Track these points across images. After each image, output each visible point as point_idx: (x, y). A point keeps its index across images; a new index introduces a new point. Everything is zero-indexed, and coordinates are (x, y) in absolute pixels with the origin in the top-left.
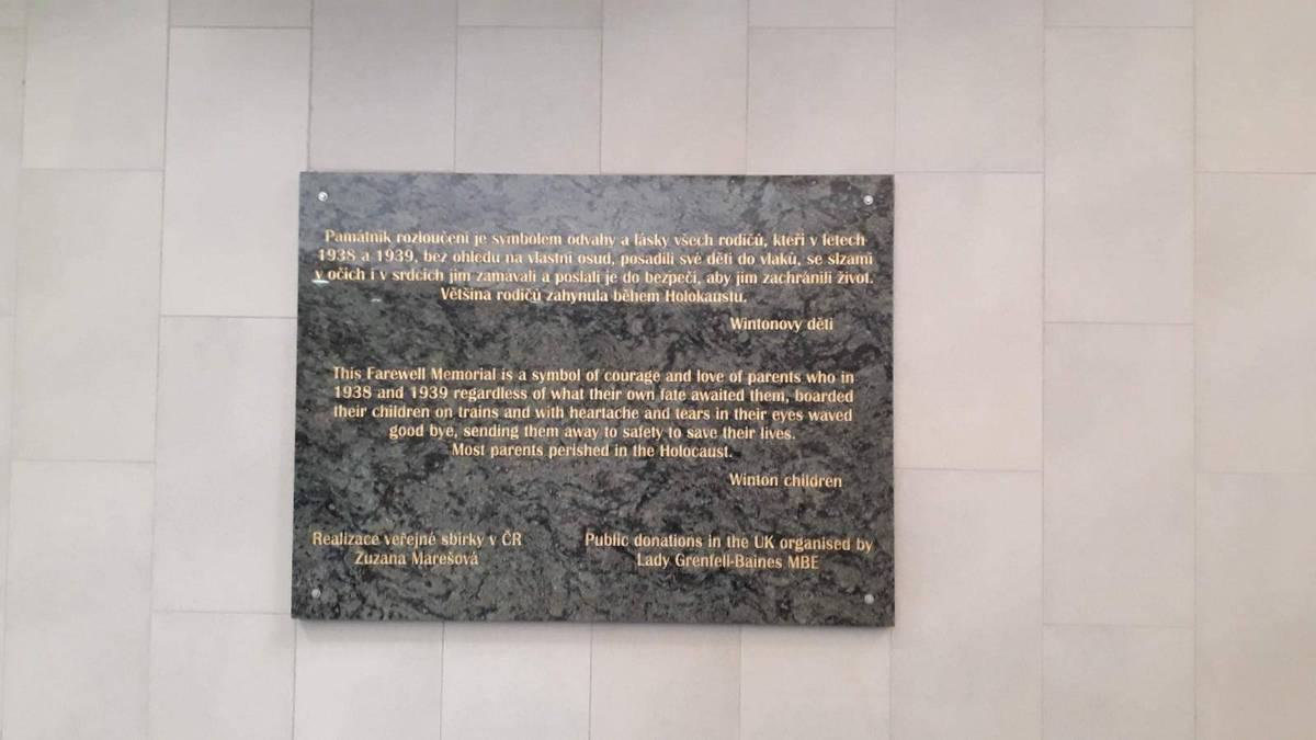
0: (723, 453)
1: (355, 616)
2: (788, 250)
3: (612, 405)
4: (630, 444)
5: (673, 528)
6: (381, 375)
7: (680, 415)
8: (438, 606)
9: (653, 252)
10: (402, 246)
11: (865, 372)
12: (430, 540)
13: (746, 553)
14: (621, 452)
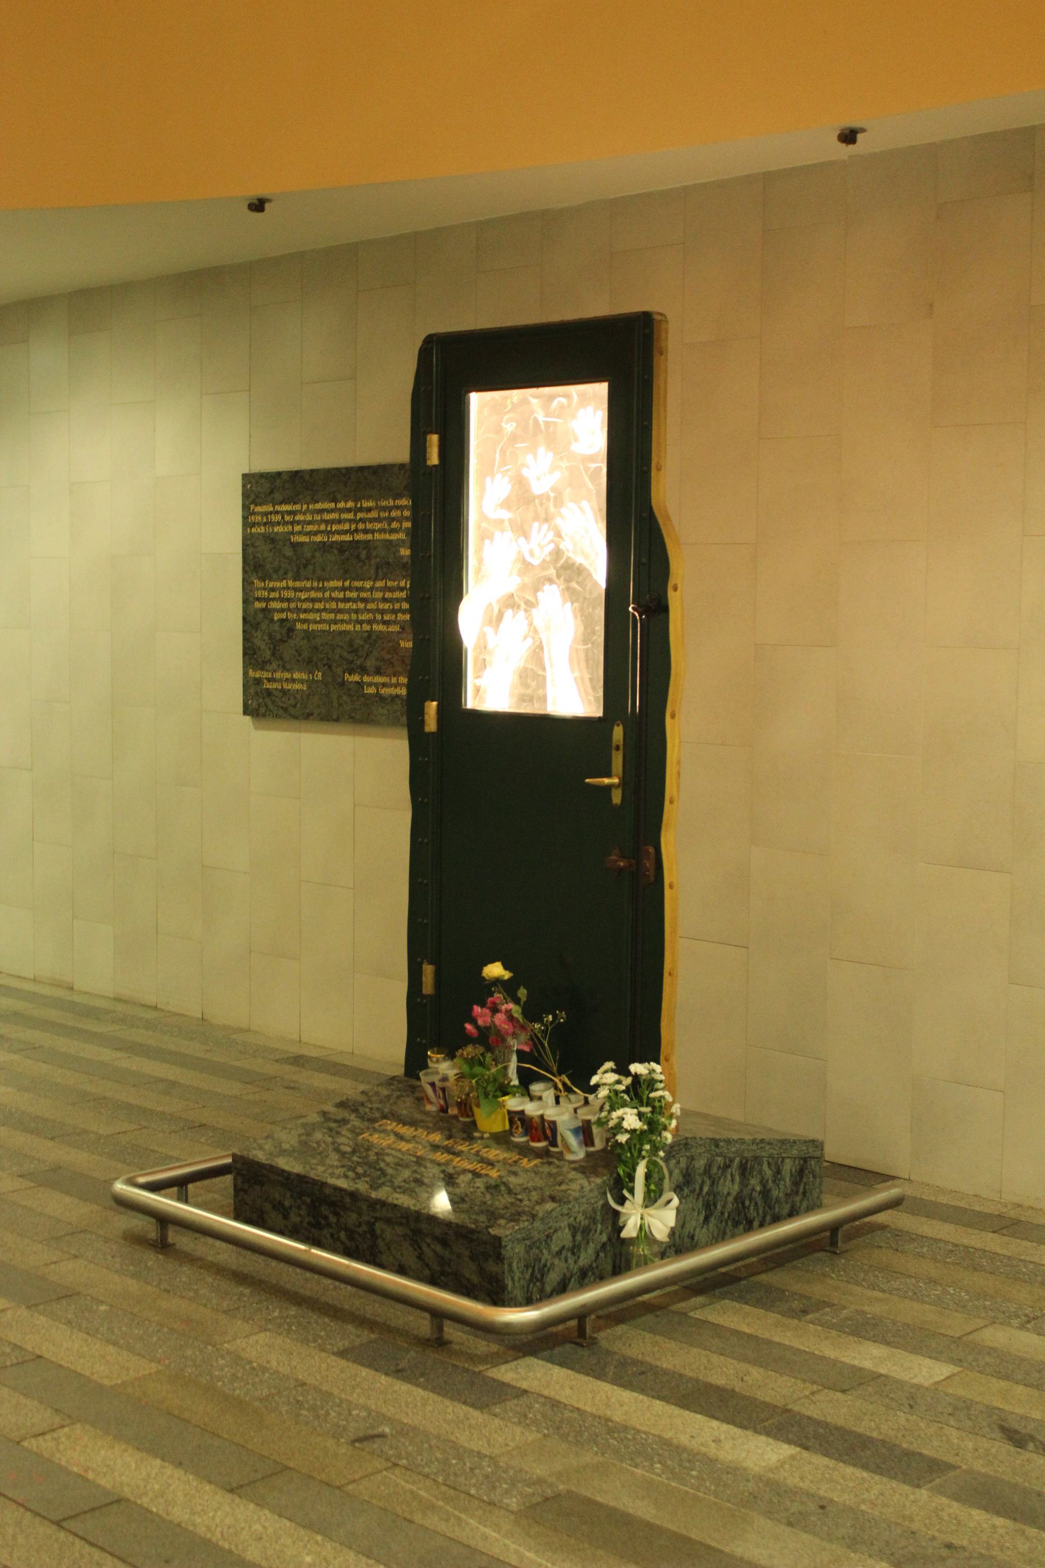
0: (397, 628)
1: (264, 715)
4: (361, 622)
5: (378, 672)
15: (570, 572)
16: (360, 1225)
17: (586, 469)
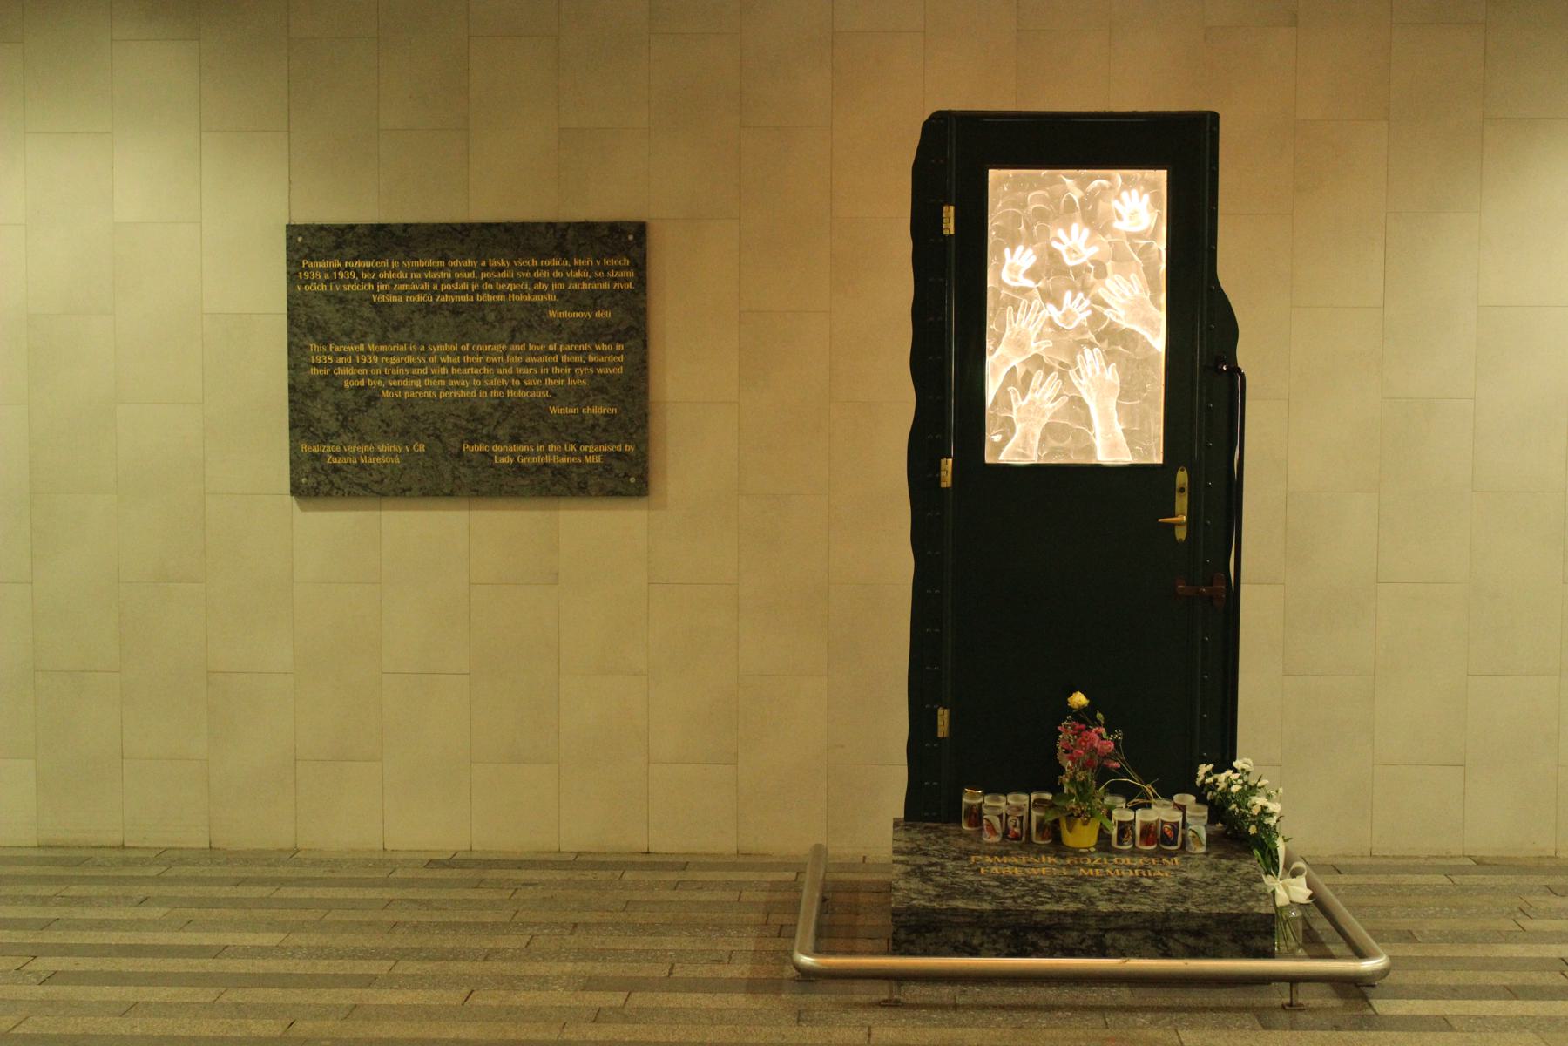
1: (328, 494)
2: (583, 268)
3: (477, 366)
4: (489, 389)
5: (516, 440)
6: (338, 349)
7: (519, 371)
8: (376, 487)
9: (501, 269)
10: (349, 269)
11: (630, 343)
12: (370, 449)
13: (560, 455)
14: (483, 394)
15: (1112, 338)
17: (1133, 246)
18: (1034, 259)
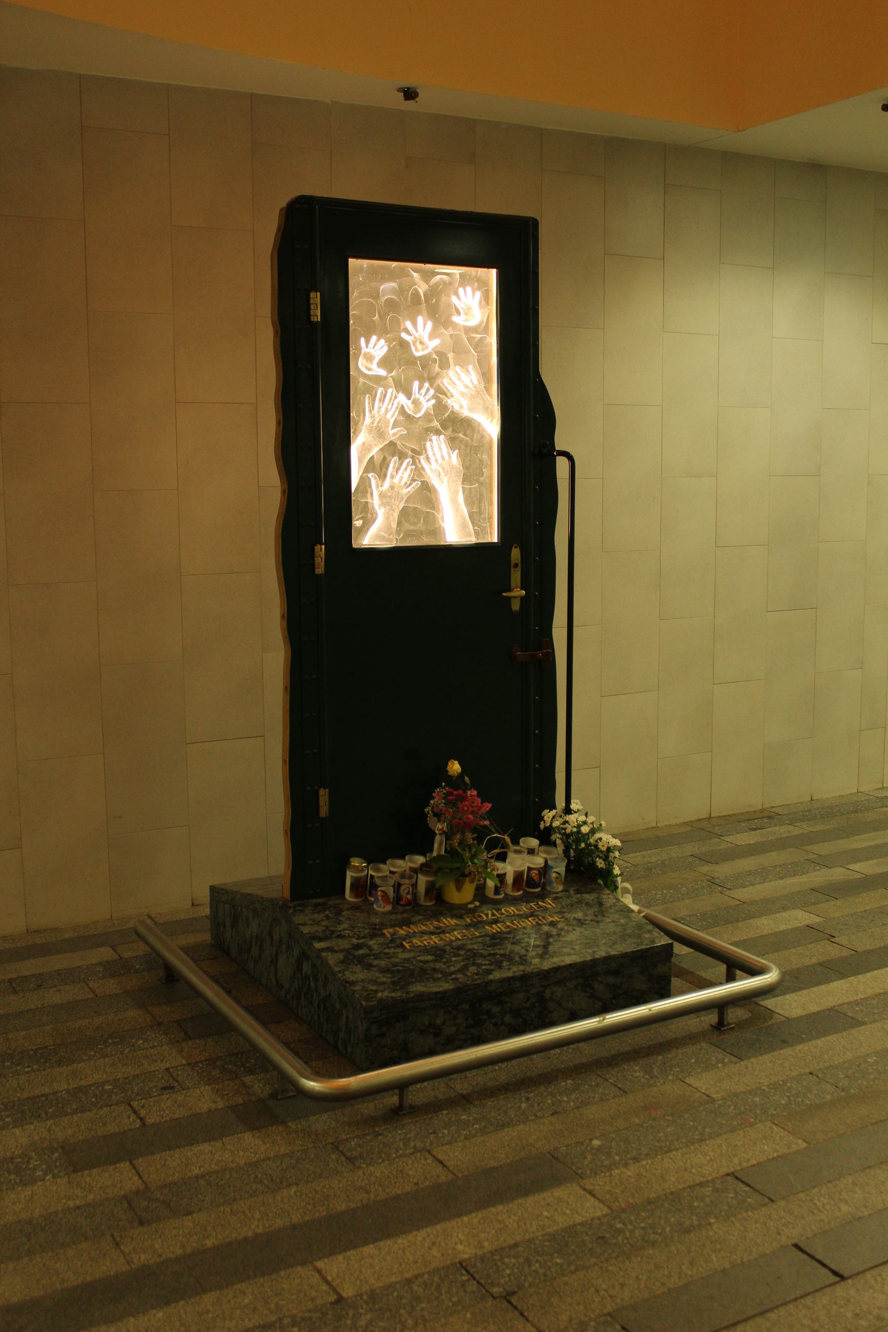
15: (456, 427)
16: (528, 999)
18: (386, 349)
